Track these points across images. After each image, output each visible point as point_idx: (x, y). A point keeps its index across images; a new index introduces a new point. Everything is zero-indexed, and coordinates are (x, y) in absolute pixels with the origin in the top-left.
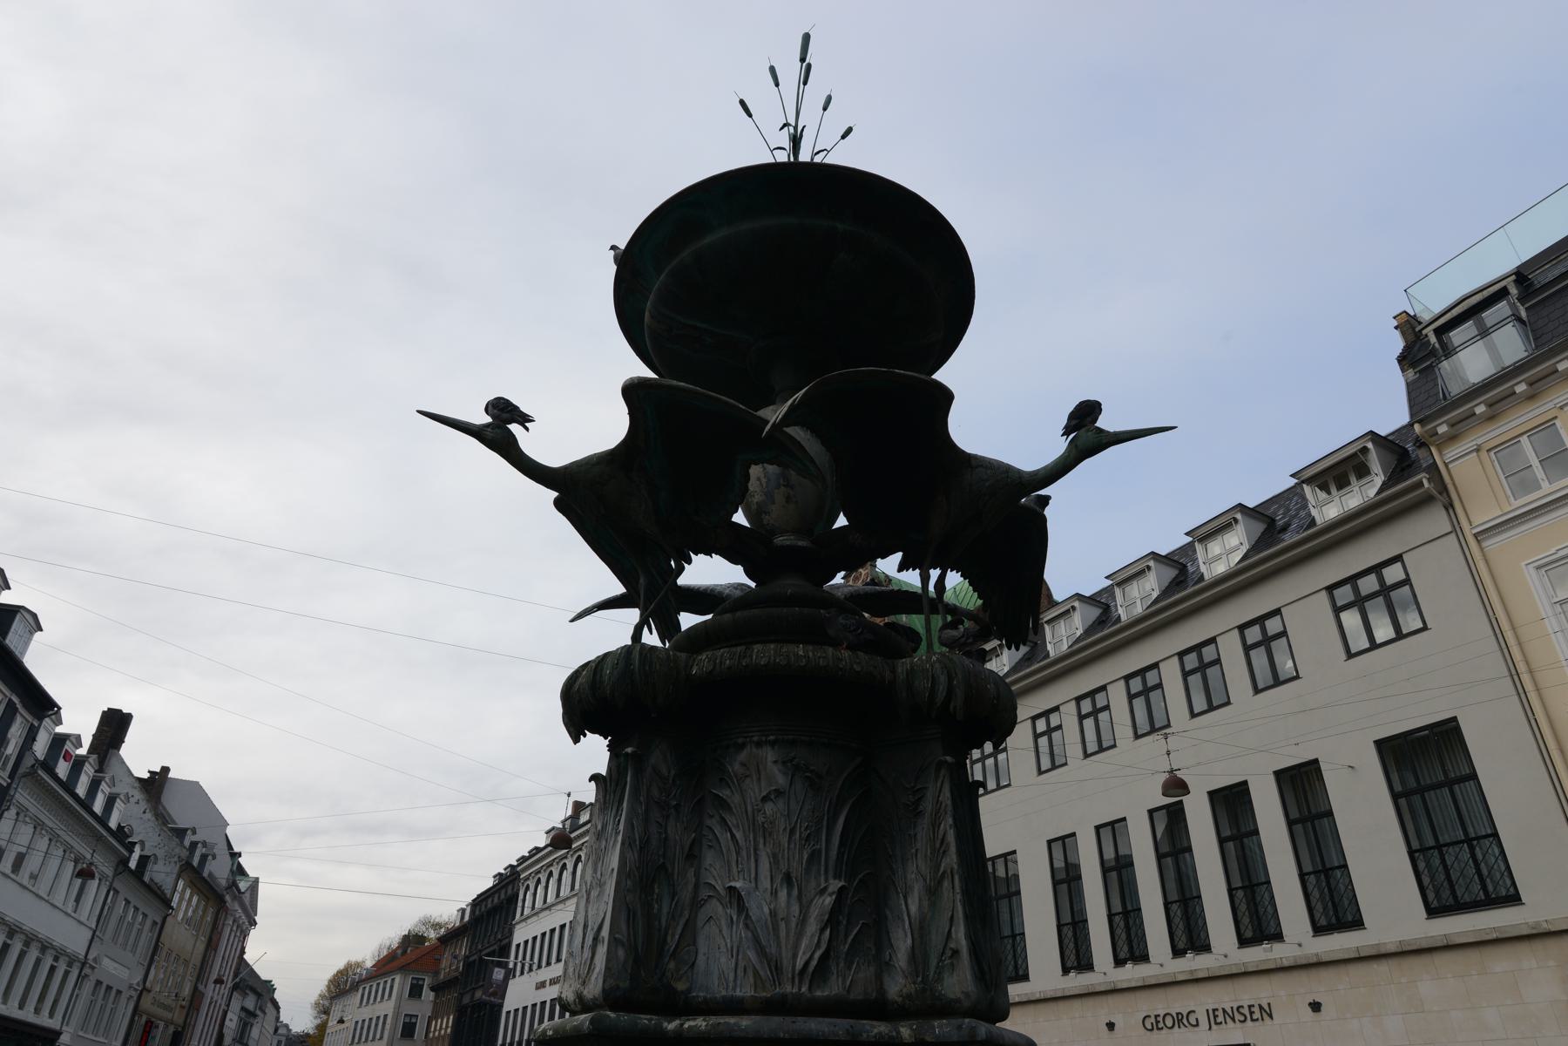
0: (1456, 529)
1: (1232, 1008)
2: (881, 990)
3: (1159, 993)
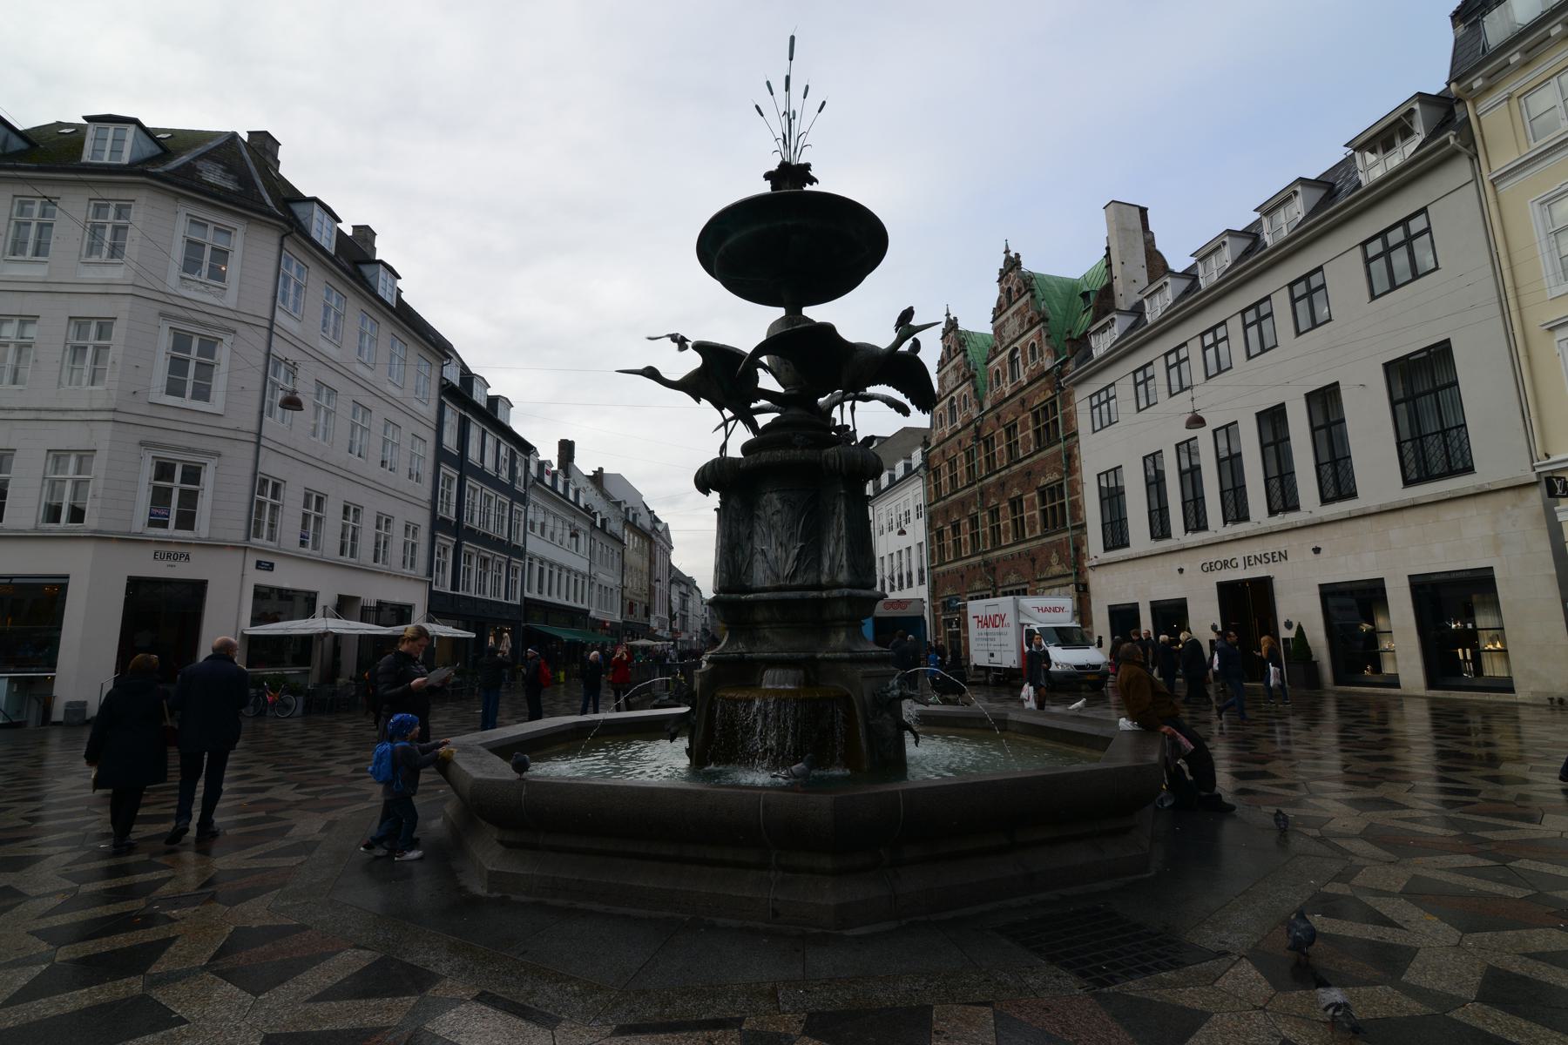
0: (1476, 178)
2: (819, 581)
3: (1214, 549)
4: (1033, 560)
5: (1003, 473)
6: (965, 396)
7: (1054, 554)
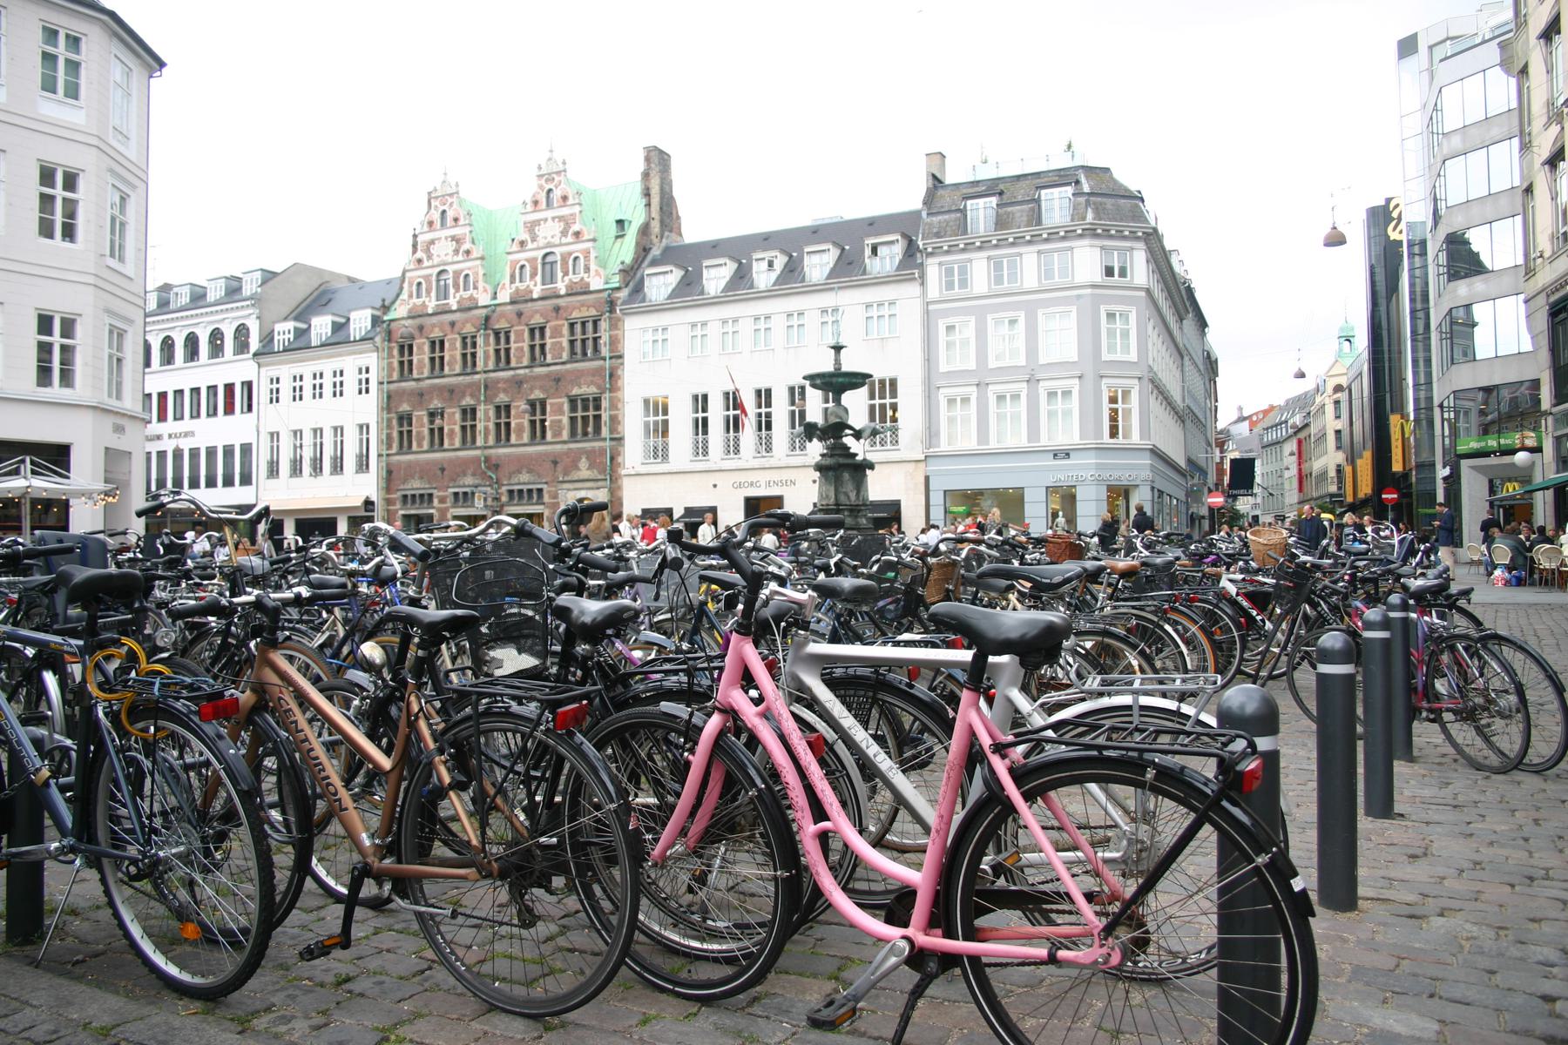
4: (555, 463)
5: (521, 372)
6: (467, 276)
7: (584, 460)
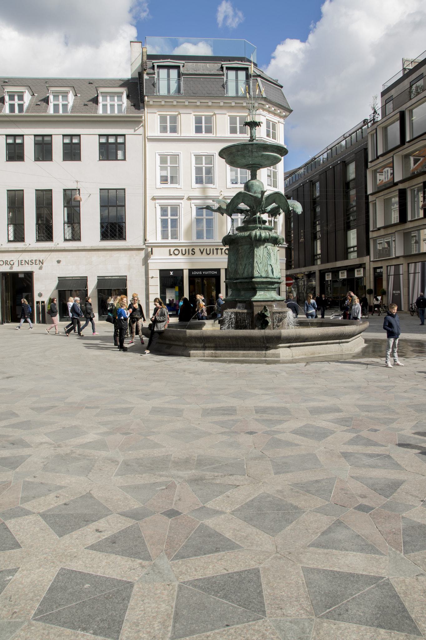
1: (28, 260)
